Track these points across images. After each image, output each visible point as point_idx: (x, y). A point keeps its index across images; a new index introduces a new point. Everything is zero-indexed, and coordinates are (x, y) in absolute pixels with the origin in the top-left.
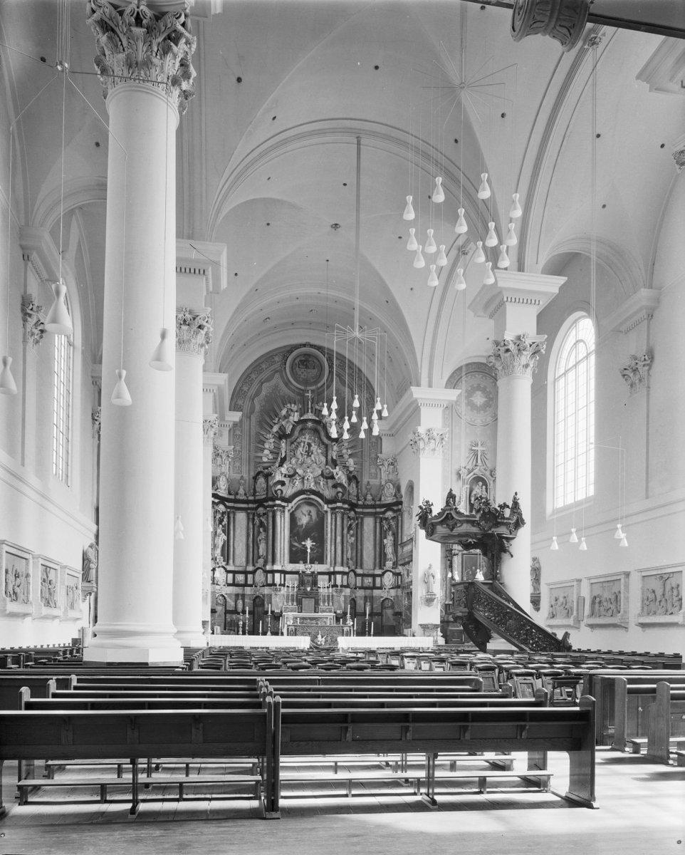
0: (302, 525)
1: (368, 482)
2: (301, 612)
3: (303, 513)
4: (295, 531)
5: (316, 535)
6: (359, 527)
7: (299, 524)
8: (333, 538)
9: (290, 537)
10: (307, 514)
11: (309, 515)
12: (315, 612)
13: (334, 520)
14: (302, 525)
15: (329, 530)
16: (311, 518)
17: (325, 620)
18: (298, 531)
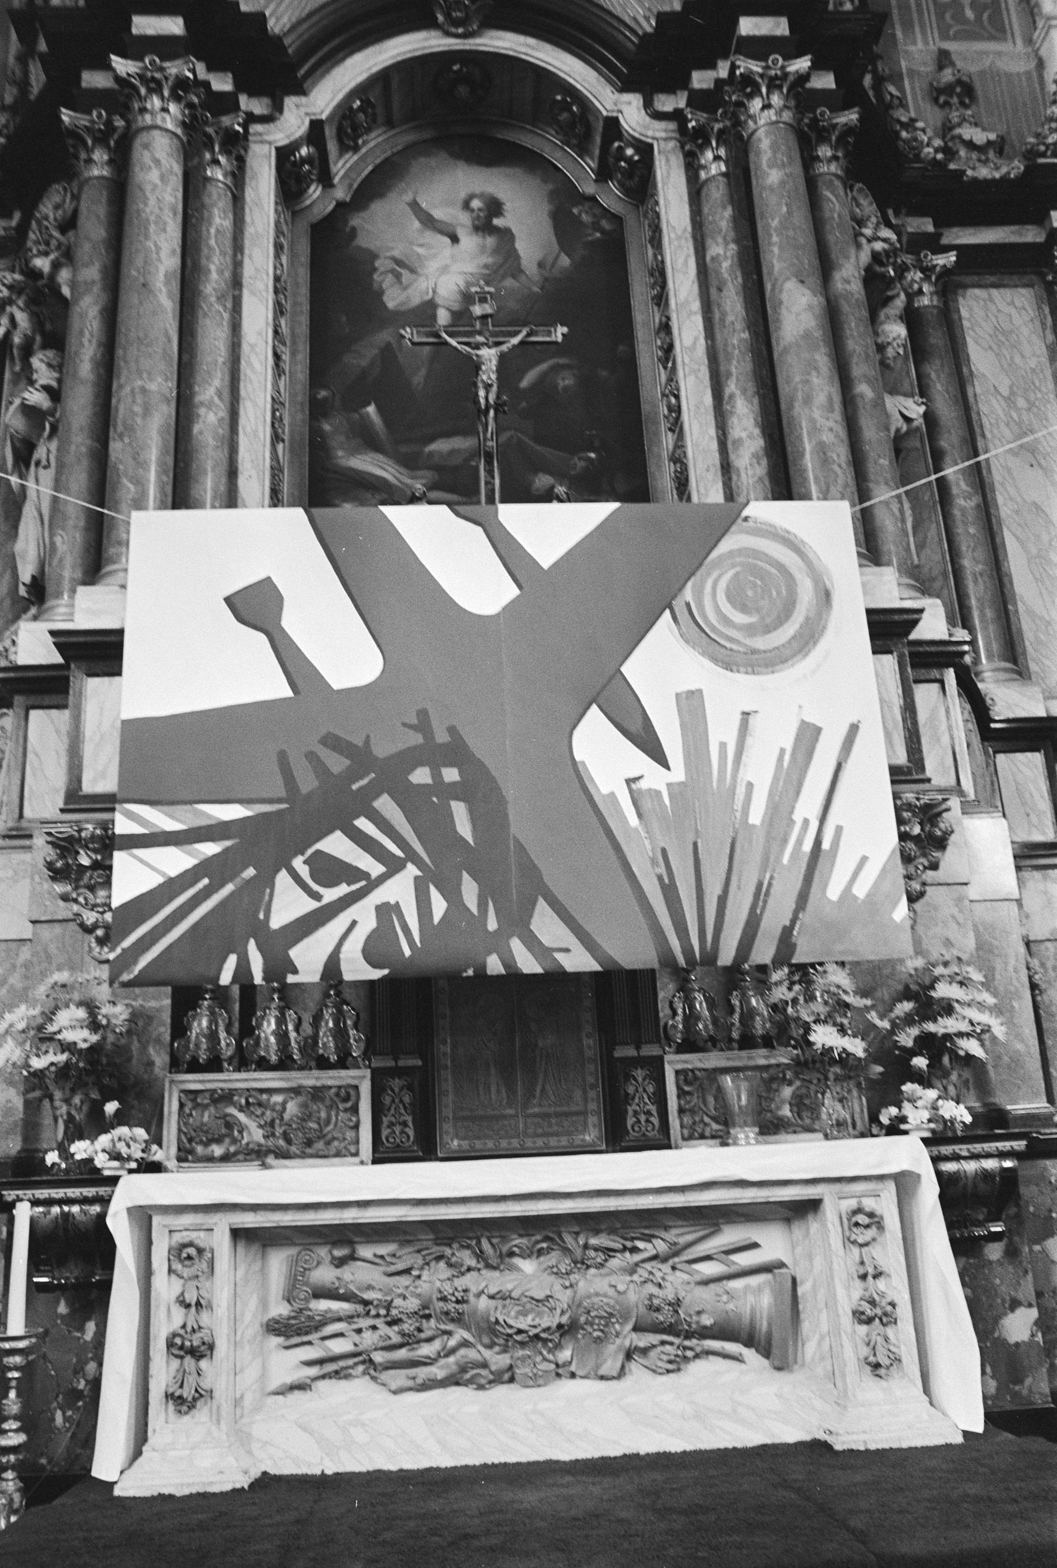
0: (430, 307)
1: (943, 59)
2: (426, 1150)
3: (429, 222)
4: (363, 356)
5: (566, 381)
6: (936, 338)
7: (393, 299)
8: (737, 336)
9: (317, 410)
10: (463, 220)
11: (484, 226)
12: (617, 1139)
13: (717, 193)
14: (430, 307)
15: (683, 286)
16: (506, 236)
17: (773, 1243)
18: (388, 353)
